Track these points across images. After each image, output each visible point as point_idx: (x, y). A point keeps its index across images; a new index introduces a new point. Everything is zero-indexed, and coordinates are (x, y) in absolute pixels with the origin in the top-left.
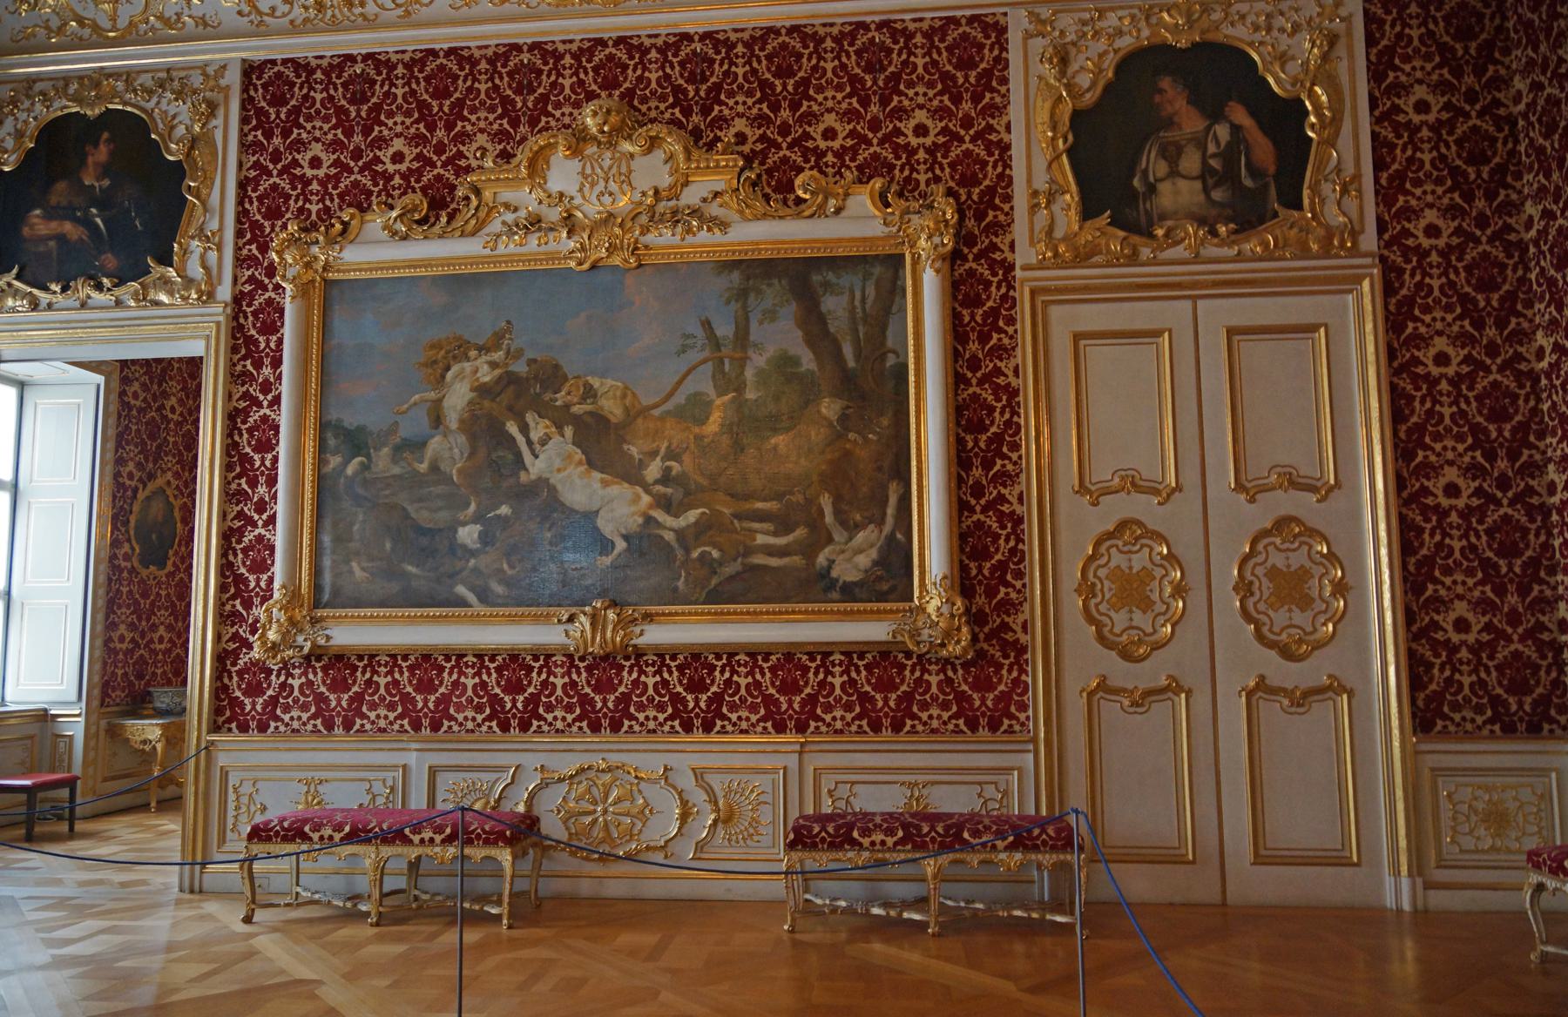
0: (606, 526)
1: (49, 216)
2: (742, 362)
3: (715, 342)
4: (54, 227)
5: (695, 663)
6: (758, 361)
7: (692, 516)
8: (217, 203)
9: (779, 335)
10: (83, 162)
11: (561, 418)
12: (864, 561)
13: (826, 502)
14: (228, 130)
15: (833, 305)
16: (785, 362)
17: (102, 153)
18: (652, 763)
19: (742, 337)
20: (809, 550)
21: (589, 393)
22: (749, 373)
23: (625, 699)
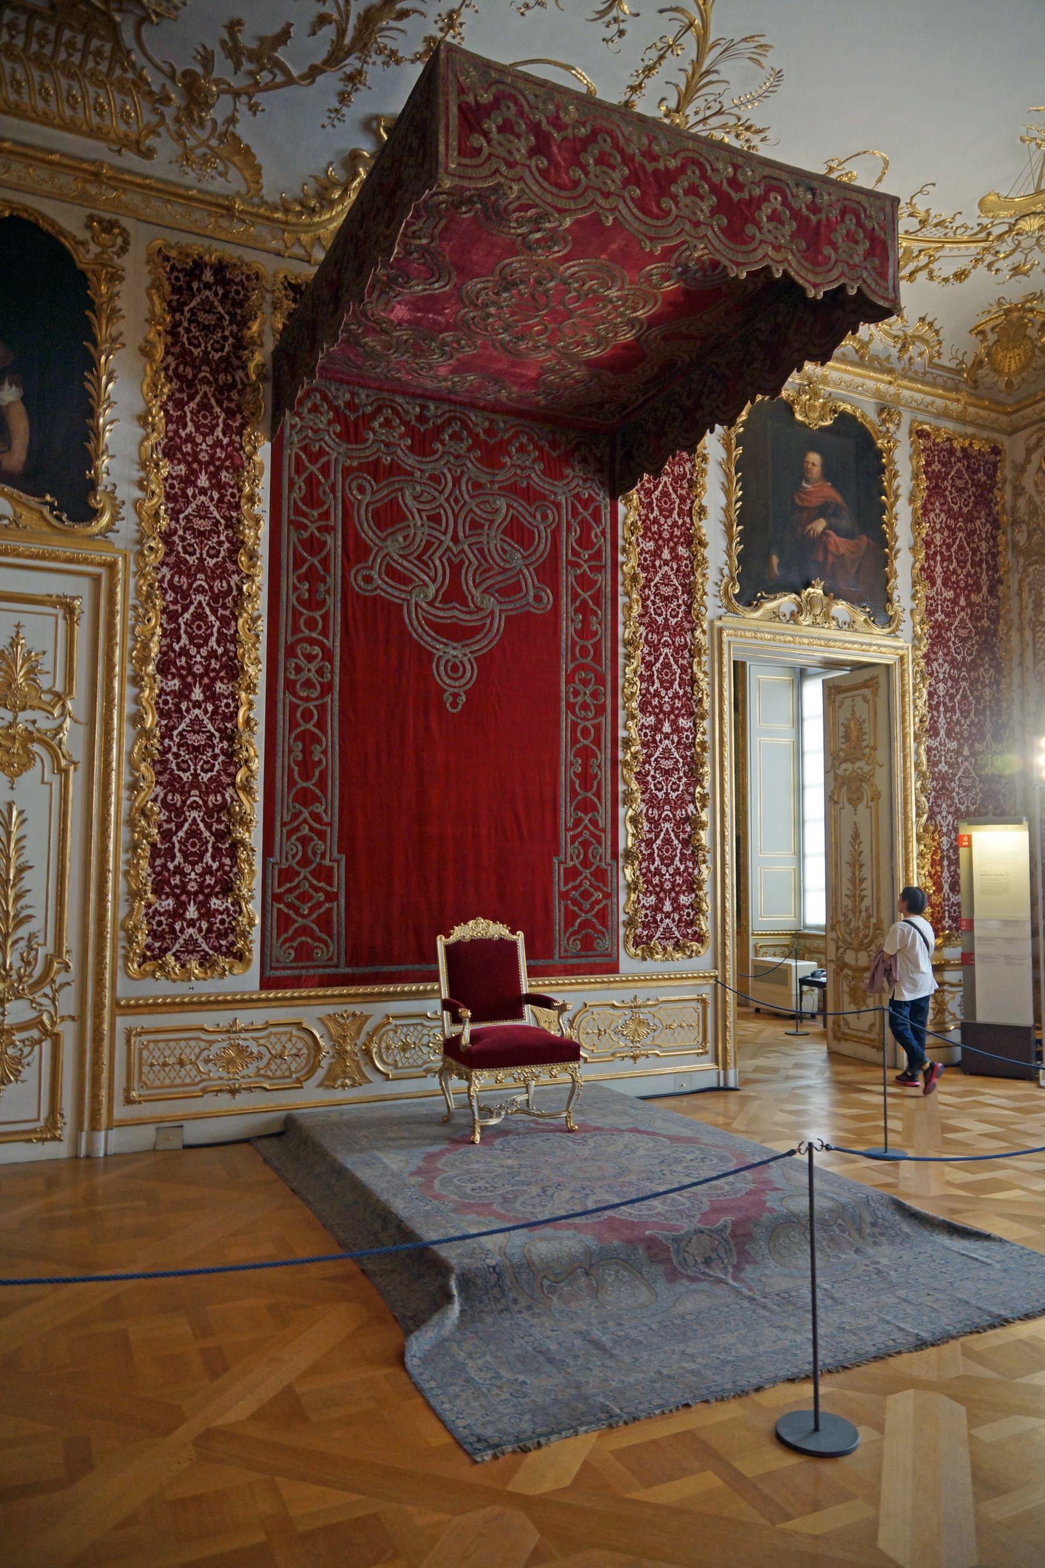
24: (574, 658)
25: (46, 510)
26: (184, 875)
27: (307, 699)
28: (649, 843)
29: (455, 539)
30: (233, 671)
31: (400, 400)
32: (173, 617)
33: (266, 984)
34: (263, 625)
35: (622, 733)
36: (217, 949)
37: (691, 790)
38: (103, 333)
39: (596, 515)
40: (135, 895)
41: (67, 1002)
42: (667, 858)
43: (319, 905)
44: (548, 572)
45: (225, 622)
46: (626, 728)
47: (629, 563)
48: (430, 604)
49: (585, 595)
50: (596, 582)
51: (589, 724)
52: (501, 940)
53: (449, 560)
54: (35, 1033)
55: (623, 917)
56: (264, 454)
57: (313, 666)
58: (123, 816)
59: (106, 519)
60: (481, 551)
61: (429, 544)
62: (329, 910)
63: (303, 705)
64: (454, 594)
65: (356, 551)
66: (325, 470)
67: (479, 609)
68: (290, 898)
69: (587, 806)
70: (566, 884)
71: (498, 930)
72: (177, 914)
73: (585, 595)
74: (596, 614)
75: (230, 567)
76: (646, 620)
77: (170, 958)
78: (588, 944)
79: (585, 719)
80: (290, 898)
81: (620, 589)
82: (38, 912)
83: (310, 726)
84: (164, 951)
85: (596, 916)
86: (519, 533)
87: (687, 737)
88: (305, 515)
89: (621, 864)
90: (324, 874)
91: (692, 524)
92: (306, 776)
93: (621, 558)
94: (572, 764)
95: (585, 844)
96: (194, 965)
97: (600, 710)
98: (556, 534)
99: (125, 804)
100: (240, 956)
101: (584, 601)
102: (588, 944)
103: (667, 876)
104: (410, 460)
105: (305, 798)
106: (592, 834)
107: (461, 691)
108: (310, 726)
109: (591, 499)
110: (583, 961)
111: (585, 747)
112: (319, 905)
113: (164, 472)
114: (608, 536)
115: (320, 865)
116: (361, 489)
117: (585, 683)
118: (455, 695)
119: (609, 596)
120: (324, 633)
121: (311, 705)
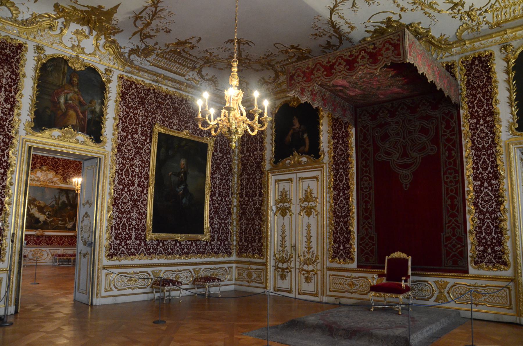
0: (40, 220)
2: (59, 201)
3: (56, 198)
5: (50, 237)
6: (61, 201)
7: (51, 219)
9: (64, 198)
11: (35, 206)
12: (71, 226)
13: (67, 219)
15: (70, 195)
16: (64, 202)
18: (44, 249)
19: (59, 198)
20: (65, 224)
21: (39, 203)
22: (60, 203)
23: (41, 241)
24: (446, 166)
25: (312, 158)
26: (340, 238)
27: (366, 192)
28: (480, 228)
29: (404, 139)
30: (348, 187)
31: (386, 104)
32: (336, 176)
33: (358, 266)
34: (355, 175)
35: (466, 189)
36: (347, 257)
37: (499, 207)
38: (320, 116)
39: (452, 118)
40: (330, 243)
41: (319, 267)
42: (488, 233)
43: (370, 247)
44: (435, 141)
45: (347, 175)
46: (468, 187)
47: (465, 129)
48: (398, 159)
49: (449, 145)
50: (452, 139)
51: (453, 188)
52: (404, 259)
53: (402, 145)
54: (314, 273)
55: (469, 254)
56: (353, 131)
57: (367, 183)
58: (328, 224)
59: (322, 156)
60: (412, 140)
61: (396, 142)
62: (373, 248)
63: (365, 193)
64: (405, 155)
65: (376, 149)
66: (368, 131)
67: (412, 158)
68: (363, 245)
69: (454, 216)
70: (446, 242)
71: (403, 255)
72: (338, 248)
73: (449, 145)
74: (454, 150)
75: (347, 161)
76: (474, 148)
77: (337, 259)
78: (455, 263)
79: (451, 186)
80: (363, 245)
81: (463, 139)
82: (313, 246)
83: (367, 199)
84: (336, 256)
85: (458, 253)
86: (424, 131)
87: (496, 187)
88: (363, 143)
89: (468, 235)
90: (371, 238)
91: (493, 108)
92: (366, 213)
93: (462, 128)
94: (447, 202)
95: (453, 229)
96: (342, 260)
97: (457, 182)
98: (437, 128)
99: (328, 222)
100: (352, 259)
101: (449, 147)
102: (455, 263)
103: (489, 240)
104: (390, 120)
105: (366, 218)
106: (456, 225)
107: (408, 183)
108: (367, 199)
109: (449, 112)
110: (454, 268)
111: (452, 196)
112: (370, 247)
113: (332, 143)
114: (457, 122)
115: (370, 236)
116: (377, 132)
117: (451, 174)
118: (406, 185)
119: (458, 142)
120: (369, 174)
121: (367, 193)
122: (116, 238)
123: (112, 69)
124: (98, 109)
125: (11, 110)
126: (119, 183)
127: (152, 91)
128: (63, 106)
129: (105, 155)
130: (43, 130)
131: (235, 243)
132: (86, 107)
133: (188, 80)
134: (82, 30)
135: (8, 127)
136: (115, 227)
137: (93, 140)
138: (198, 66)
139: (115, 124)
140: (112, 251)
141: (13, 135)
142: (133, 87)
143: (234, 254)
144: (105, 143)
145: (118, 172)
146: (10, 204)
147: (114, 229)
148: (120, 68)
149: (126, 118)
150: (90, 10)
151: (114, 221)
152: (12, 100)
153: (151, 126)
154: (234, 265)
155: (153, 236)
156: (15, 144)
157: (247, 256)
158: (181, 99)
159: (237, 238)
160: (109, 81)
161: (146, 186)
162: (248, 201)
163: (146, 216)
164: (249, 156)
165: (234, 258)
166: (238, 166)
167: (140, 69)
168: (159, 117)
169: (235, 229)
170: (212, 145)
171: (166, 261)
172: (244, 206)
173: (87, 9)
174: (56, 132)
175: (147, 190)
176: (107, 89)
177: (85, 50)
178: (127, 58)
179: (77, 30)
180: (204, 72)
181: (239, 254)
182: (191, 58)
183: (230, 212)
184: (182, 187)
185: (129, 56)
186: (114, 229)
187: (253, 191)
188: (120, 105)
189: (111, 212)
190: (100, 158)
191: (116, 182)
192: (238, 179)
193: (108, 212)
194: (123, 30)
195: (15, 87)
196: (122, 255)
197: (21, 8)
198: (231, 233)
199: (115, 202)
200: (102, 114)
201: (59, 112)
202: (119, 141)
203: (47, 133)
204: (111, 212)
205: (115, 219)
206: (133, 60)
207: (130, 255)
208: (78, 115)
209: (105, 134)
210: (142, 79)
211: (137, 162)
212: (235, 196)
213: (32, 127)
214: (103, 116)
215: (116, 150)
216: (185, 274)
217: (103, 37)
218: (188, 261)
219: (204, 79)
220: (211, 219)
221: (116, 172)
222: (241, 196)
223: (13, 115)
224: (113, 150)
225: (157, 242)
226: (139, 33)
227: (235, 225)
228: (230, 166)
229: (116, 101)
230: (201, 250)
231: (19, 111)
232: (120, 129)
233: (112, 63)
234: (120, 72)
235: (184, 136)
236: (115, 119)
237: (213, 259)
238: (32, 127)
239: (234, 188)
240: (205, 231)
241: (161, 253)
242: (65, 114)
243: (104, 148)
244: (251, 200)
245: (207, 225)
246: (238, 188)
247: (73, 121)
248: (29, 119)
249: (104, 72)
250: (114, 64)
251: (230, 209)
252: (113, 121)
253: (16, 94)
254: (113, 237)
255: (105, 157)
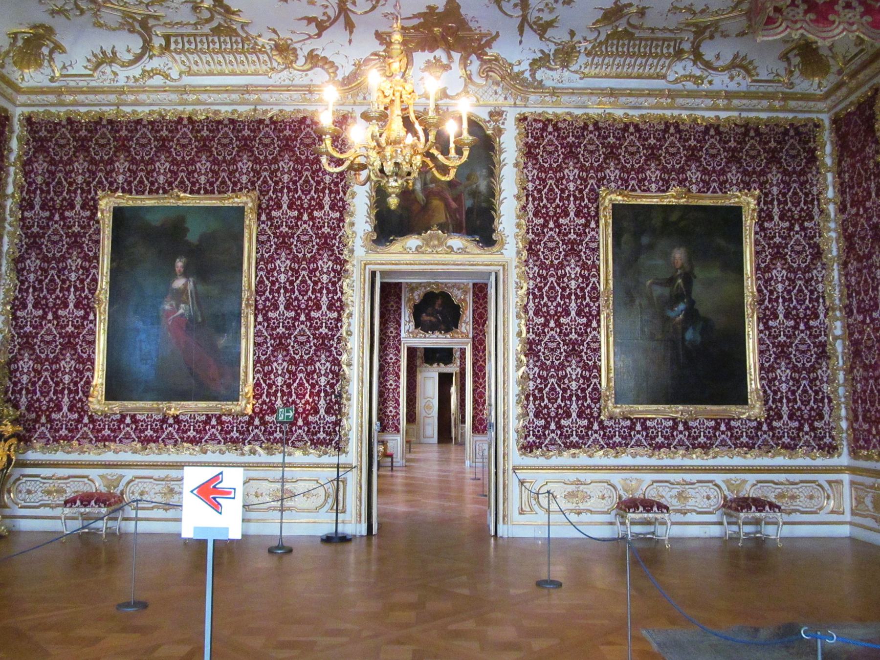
1: (427, 315)
4: (428, 318)
8: (468, 315)
10: (435, 304)
14: (470, 298)
17: (439, 302)
122: (537, 416)
123: (503, 109)
124: (483, 186)
125: (341, 220)
126: (536, 313)
127: (591, 128)
128: (421, 196)
129: (504, 266)
130: (391, 241)
131: (844, 424)
132: (461, 188)
133: (676, 81)
134: (435, 58)
135: (338, 247)
136: (534, 395)
137: (478, 242)
138: (686, 46)
139: (519, 206)
140: (531, 439)
141: (347, 258)
142: (550, 129)
143: (845, 451)
144: (503, 244)
145: (534, 294)
146: (349, 365)
147: (531, 398)
148: (518, 102)
149: (539, 191)
150: (422, 20)
151: (531, 383)
152: (340, 204)
153: (595, 198)
154: (846, 478)
155: (618, 410)
156: (350, 271)
157: (868, 458)
158: (663, 127)
159: (847, 414)
160: (499, 132)
161: (594, 313)
162: (863, 322)
163: (599, 371)
164: (857, 214)
165: (843, 459)
166: (837, 243)
167: (554, 92)
168: (612, 172)
169: (841, 391)
170: (752, 206)
171: (654, 461)
172: (856, 336)
173: (416, 22)
174: (413, 241)
175: (599, 322)
176: (497, 148)
177: (448, 92)
178: (530, 79)
179: (428, 62)
180: (708, 52)
181: (854, 453)
182: (659, 35)
183: (824, 351)
184: (682, 306)
185: (533, 75)
186: (531, 398)
187: (871, 299)
188: (525, 170)
189: (523, 369)
190: (496, 273)
191: (531, 313)
192: (840, 274)
193: (518, 367)
194: (498, 33)
195: (343, 183)
196: (550, 447)
197: (337, 60)
198: (830, 401)
199: (531, 349)
200: (492, 193)
201: (415, 208)
202: (531, 236)
203: (397, 246)
204: (523, 369)
205: (534, 380)
206: (542, 81)
207: (568, 448)
208: (447, 206)
209: (500, 228)
210: (567, 110)
211: (572, 269)
212: (838, 313)
213: (374, 241)
214: (493, 196)
215: (525, 253)
216: (704, 490)
217: (473, 57)
218: (710, 462)
219: (715, 69)
220: (766, 370)
221: (528, 294)
222: (850, 313)
223: (343, 226)
224: (519, 253)
225: (628, 423)
226: (526, 24)
227: (841, 382)
228: (817, 246)
229: (516, 165)
230: (744, 439)
231: (353, 219)
232: (531, 214)
233: (502, 99)
234: (519, 110)
235: (674, 202)
236: (518, 198)
237: (781, 461)
238: (374, 241)
239: (831, 296)
240: (752, 397)
241: (639, 444)
242: (426, 208)
243: (502, 254)
244: (868, 321)
245: (753, 383)
246: (842, 296)
247: (441, 216)
248: (369, 228)
249: (488, 119)
250: (506, 98)
251: (823, 345)
252: (515, 202)
253: (345, 194)
254: (531, 414)
255: (504, 269)
